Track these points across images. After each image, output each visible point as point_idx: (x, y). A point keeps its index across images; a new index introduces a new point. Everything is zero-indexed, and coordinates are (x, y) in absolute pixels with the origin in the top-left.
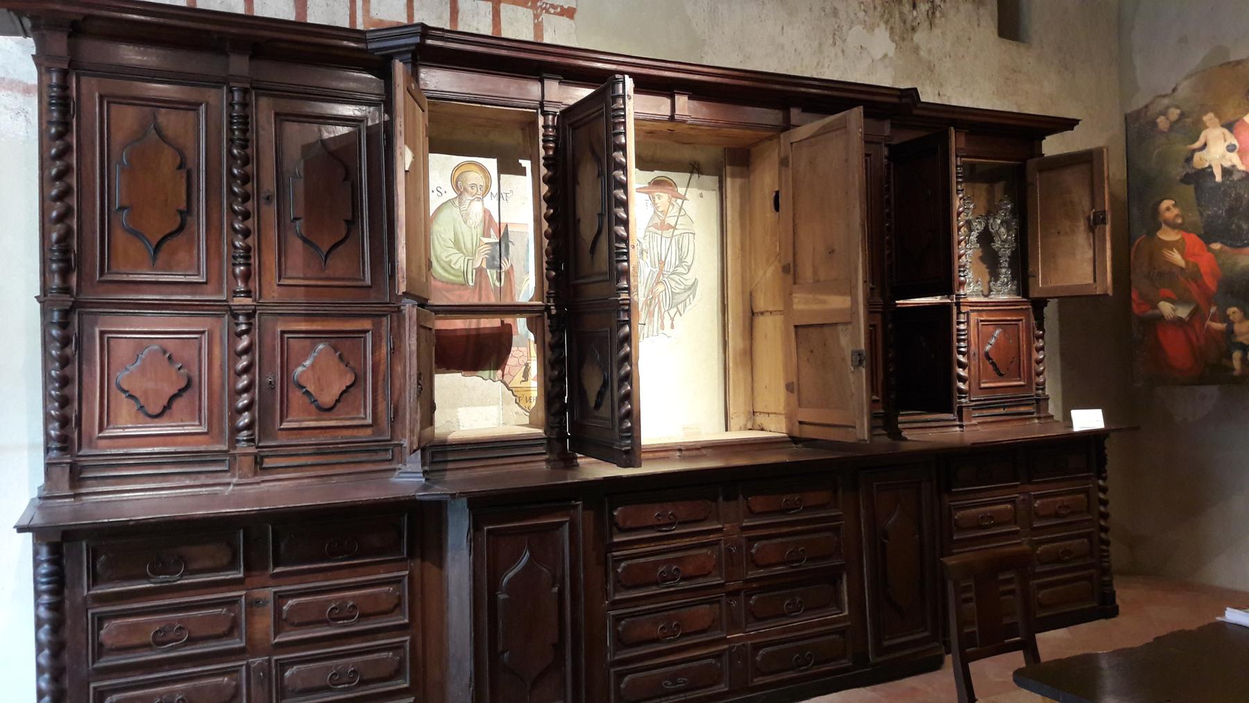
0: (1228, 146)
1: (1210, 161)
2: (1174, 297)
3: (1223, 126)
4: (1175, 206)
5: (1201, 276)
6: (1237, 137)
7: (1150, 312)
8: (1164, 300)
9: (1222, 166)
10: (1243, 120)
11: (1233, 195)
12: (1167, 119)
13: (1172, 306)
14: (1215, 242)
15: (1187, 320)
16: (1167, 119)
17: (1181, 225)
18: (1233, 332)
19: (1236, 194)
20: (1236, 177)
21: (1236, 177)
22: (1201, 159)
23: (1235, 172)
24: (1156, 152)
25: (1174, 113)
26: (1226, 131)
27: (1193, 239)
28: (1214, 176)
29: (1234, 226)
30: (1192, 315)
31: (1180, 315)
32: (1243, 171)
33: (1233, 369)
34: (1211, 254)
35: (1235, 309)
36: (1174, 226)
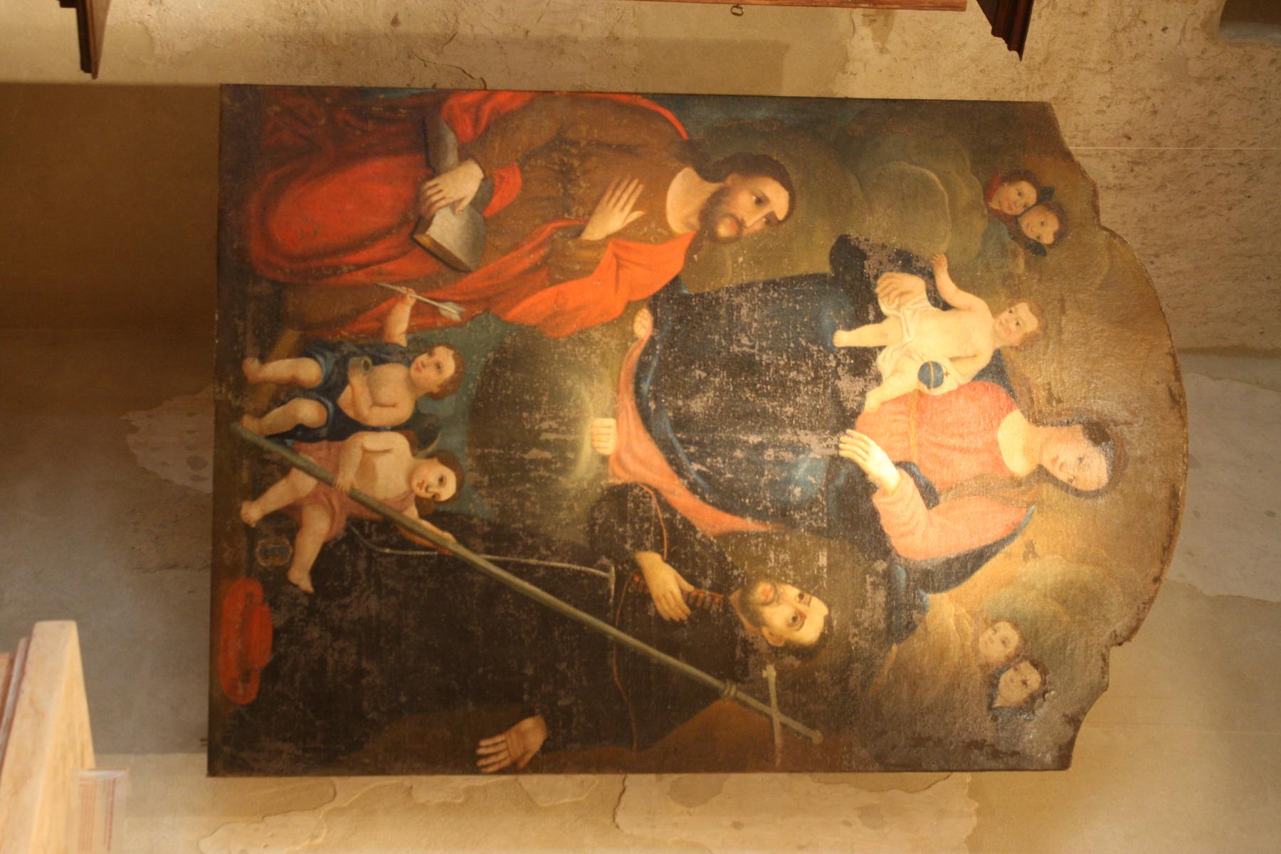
0: (937, 366)
1: (898, 318)
2: (497, 203)
3: (997, 355)
4: (770, 220)
5: (554, 282)
6: (960, 388)
7: (451, 139)
8: (484, 180)
9: (881, 348)
10: (1010, 409)
11: (793, 374)
12: (1027, 209)
13: (466, 203)
14: (657, 324)
15: (423, 239)
16: (1027, 209)
17: (714, 237)
18: (379, 361)
19: (796, 383)
20: (846, 384)
21: (846, 384)
22: (902, 294)
23: (859, 384)
24: (928, 172)
25: (1043, 228)
26: (984, 360)
27: (670, 263)
28: (849, 328)
29: (699, 373)
30: (438, 254)
31: (437, 220)
32: (861, 405)
33: (264, 359)
34: (619, 309)
35: (450, 368)
36: (708, 214)
